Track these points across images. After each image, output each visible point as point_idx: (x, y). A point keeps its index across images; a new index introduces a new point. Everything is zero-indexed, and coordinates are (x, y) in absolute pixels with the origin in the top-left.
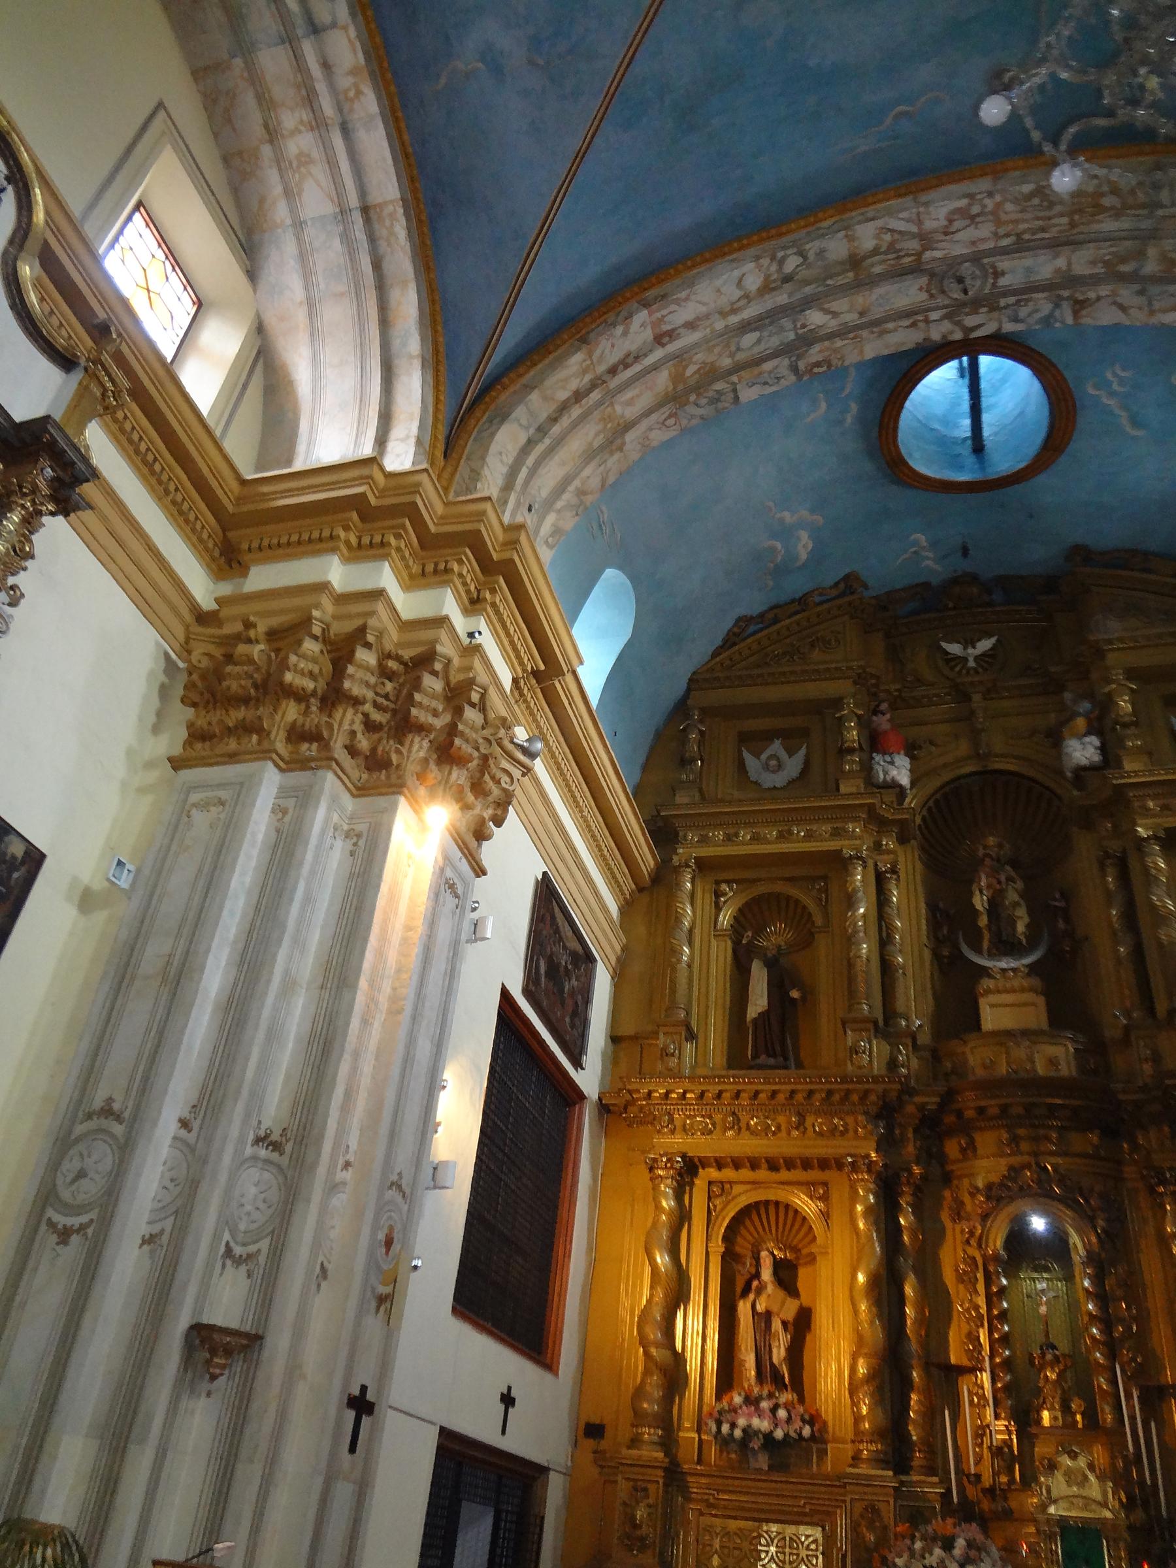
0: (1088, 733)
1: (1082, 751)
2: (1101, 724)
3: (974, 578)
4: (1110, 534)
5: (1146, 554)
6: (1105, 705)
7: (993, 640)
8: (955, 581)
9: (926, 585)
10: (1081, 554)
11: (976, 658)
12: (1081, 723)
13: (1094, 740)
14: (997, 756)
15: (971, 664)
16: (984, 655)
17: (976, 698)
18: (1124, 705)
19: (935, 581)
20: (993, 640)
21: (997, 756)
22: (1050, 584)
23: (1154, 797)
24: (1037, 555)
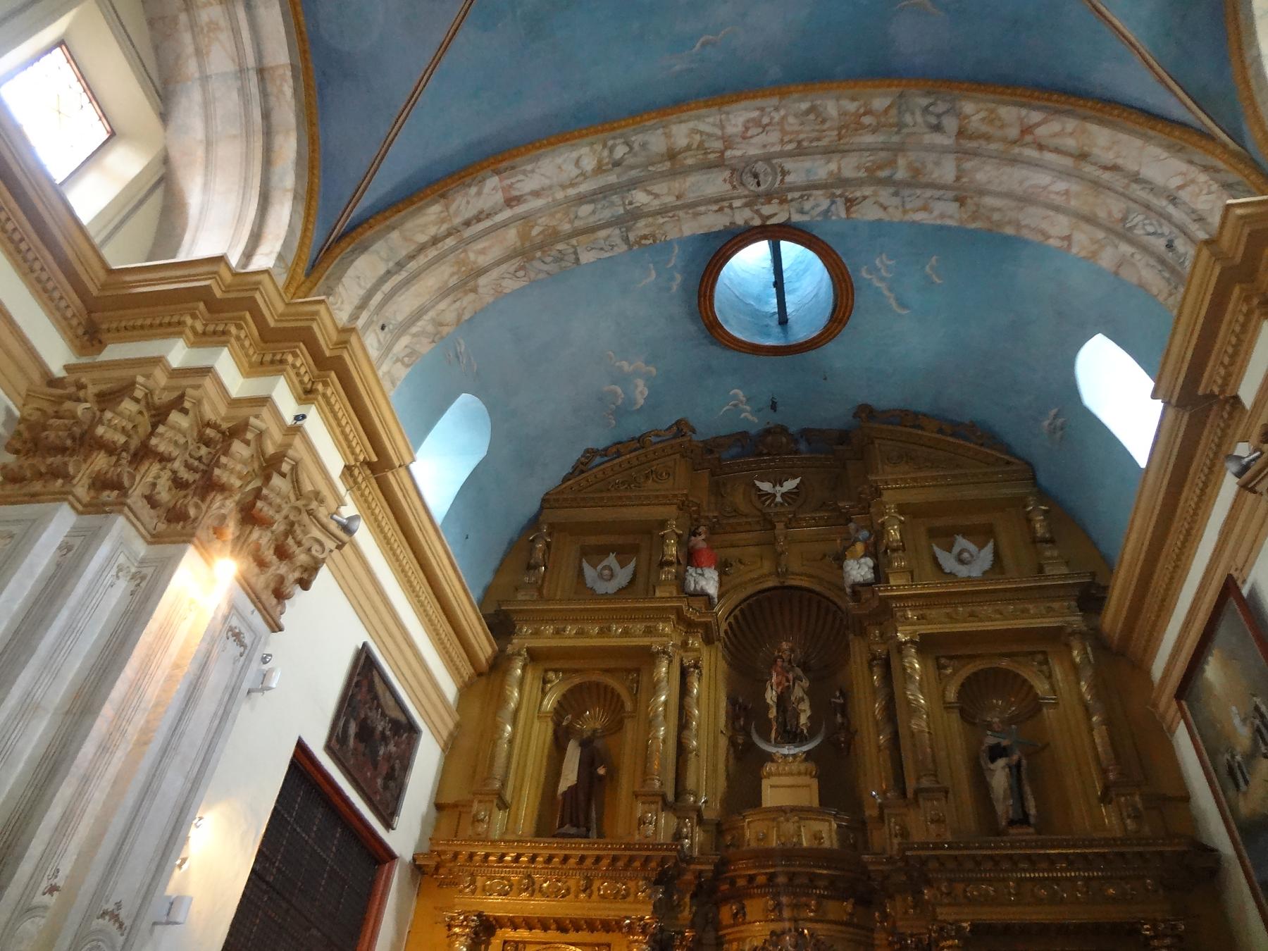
0: (865, 556)
1: (859, 570)
2: (878, 551)
3: (783, 430)
4: (887, 397)
5: (916, 414)
6: (879, 533)
7: (798, 481)
8: (768, 432)
9: (744, 434)
10: (866, 412)
11: (783, 495)
12: (859, 547)
13: (870, 562)
14: (793, 574)
15: (779, 499)
16: (789, 493)
17: (780, 526)
18: (894, 533)
19: (753, 431)
20: (798, 481)
21: (793, 574)
22: (843, 437)
23: (914, 608)
24: (832, 413)
